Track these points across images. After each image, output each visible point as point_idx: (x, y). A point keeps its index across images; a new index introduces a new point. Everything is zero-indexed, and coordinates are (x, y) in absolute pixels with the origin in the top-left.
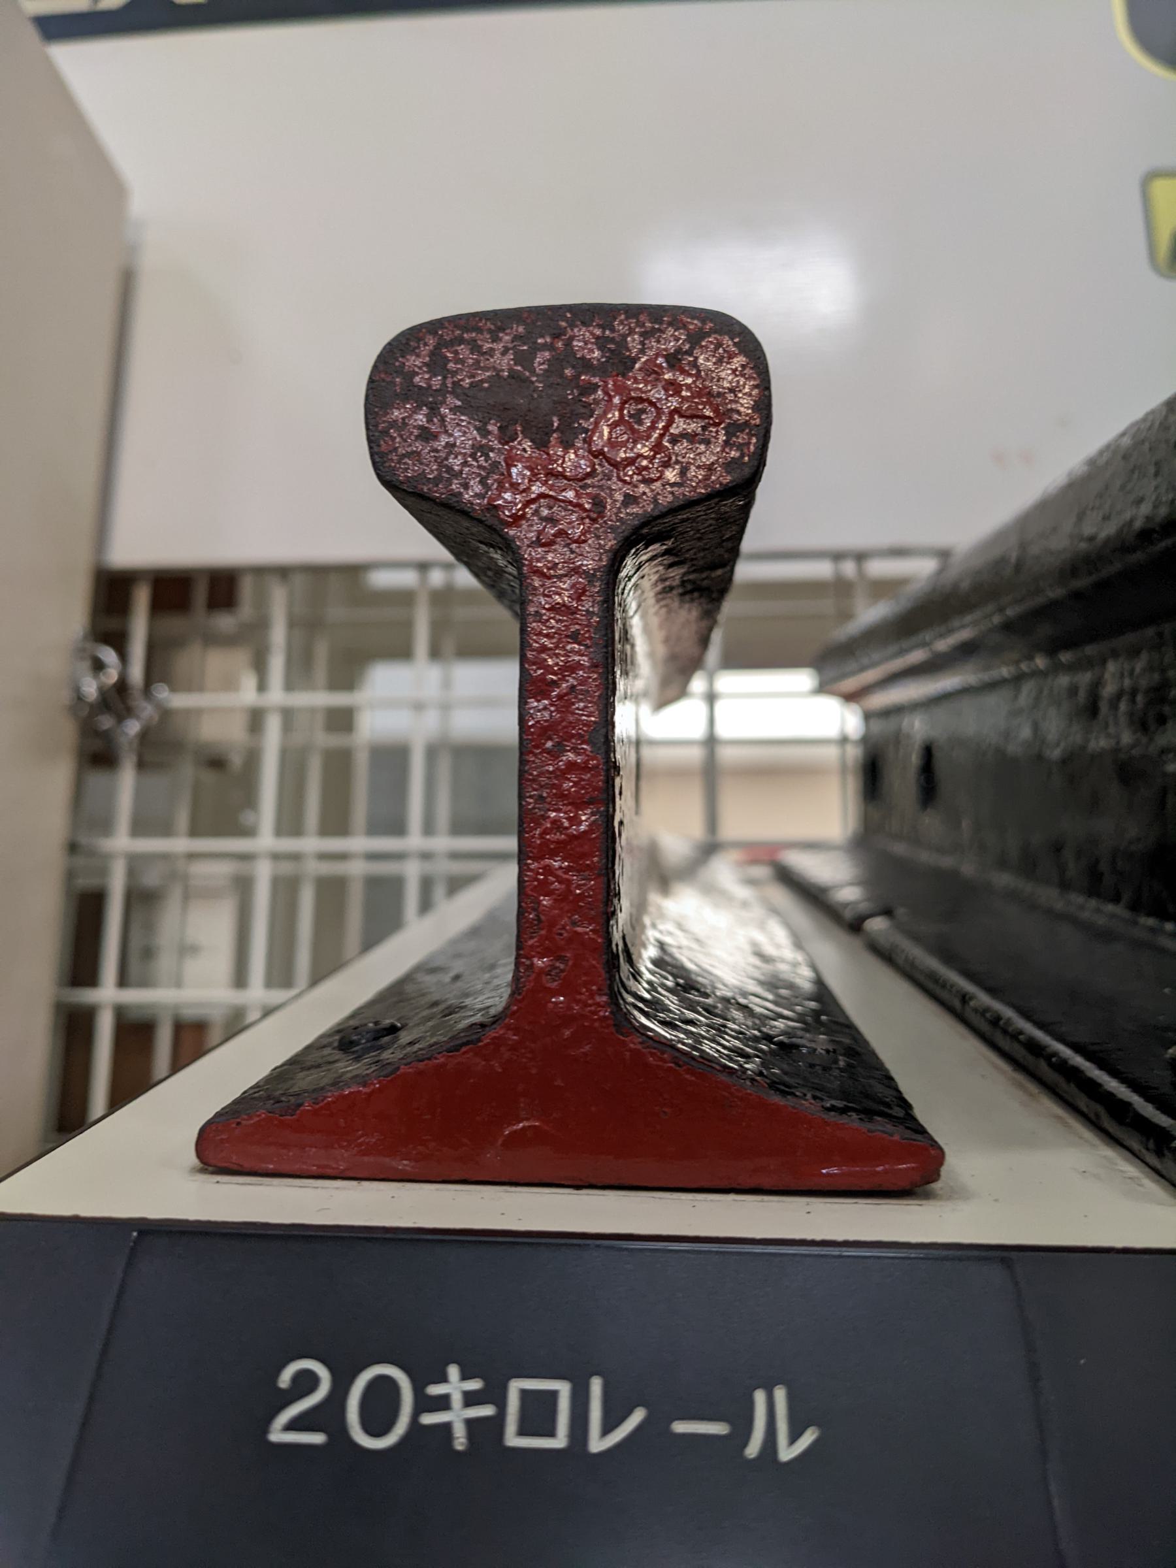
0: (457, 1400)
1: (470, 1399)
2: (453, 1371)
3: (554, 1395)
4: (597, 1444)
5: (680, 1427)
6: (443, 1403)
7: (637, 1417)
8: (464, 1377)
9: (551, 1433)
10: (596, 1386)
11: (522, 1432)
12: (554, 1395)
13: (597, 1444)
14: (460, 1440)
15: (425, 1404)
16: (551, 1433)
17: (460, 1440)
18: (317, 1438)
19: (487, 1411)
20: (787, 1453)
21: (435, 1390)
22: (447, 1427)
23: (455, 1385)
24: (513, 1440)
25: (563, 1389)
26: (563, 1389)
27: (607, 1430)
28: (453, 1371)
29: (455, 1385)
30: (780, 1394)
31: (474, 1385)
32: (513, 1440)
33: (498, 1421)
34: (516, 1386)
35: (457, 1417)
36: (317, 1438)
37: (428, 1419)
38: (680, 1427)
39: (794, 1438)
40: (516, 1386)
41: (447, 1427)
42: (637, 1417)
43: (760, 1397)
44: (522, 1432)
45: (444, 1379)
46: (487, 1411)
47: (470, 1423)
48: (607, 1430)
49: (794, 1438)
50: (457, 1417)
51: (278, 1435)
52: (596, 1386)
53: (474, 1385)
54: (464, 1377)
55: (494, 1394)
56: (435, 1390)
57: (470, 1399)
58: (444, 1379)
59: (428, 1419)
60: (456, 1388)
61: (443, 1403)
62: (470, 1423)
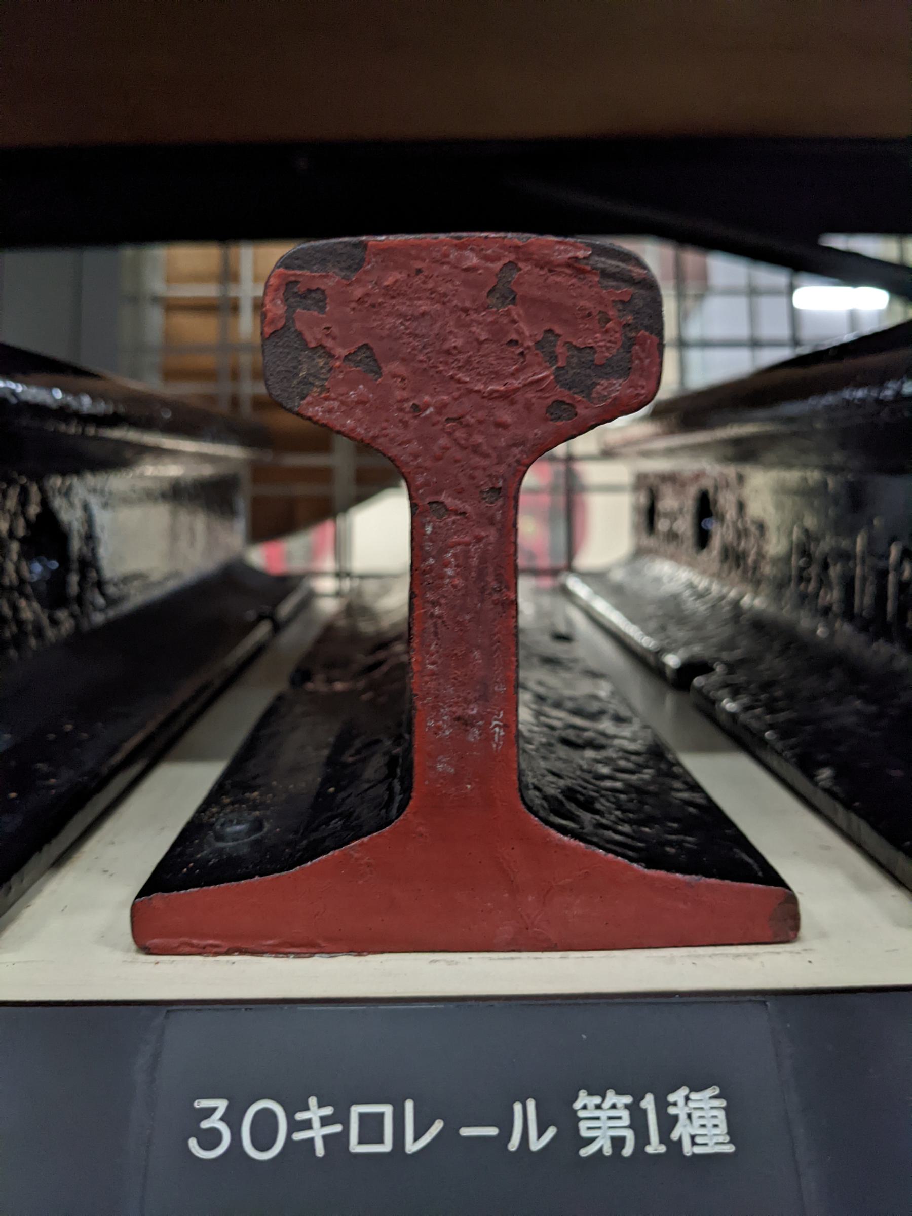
0: (316, 1123)
2: (313, 1101)
6: (307, 1125)
8: (321, 1105)
11: (361, 1141)
12: (381, 1115)
14: (320, 1151)
15: (295, 1126)
17: (320, 1151)
19: (337, 1128)
21: (300, 1116)
22: (311, 1141)
23: (315, 1112)
24: (355, 1147)
25: (387, 1110)
26: (387, 1110)
28: (313, 1101)
29: (315, 1112)
31: (328, 1111)
32: (355, 1147)
34: (356, 1111)
35: (317, 1133)
37: (298, 1136)
40: (356, 1111)
41: (311, 1141)
44: (361, 1141)
45: (306, 1108)
46: (337, 1128)
47: (326, 1138)
50: (317, 1133)
53: (328, 1111)
54: (321, 1105)
55: (341, 1117)
56: (300, 1116)
58: (306, 1108)
59: (298, 1136)
60: (315, 1114)
61: (307, 1125)
62: (326, 1138)
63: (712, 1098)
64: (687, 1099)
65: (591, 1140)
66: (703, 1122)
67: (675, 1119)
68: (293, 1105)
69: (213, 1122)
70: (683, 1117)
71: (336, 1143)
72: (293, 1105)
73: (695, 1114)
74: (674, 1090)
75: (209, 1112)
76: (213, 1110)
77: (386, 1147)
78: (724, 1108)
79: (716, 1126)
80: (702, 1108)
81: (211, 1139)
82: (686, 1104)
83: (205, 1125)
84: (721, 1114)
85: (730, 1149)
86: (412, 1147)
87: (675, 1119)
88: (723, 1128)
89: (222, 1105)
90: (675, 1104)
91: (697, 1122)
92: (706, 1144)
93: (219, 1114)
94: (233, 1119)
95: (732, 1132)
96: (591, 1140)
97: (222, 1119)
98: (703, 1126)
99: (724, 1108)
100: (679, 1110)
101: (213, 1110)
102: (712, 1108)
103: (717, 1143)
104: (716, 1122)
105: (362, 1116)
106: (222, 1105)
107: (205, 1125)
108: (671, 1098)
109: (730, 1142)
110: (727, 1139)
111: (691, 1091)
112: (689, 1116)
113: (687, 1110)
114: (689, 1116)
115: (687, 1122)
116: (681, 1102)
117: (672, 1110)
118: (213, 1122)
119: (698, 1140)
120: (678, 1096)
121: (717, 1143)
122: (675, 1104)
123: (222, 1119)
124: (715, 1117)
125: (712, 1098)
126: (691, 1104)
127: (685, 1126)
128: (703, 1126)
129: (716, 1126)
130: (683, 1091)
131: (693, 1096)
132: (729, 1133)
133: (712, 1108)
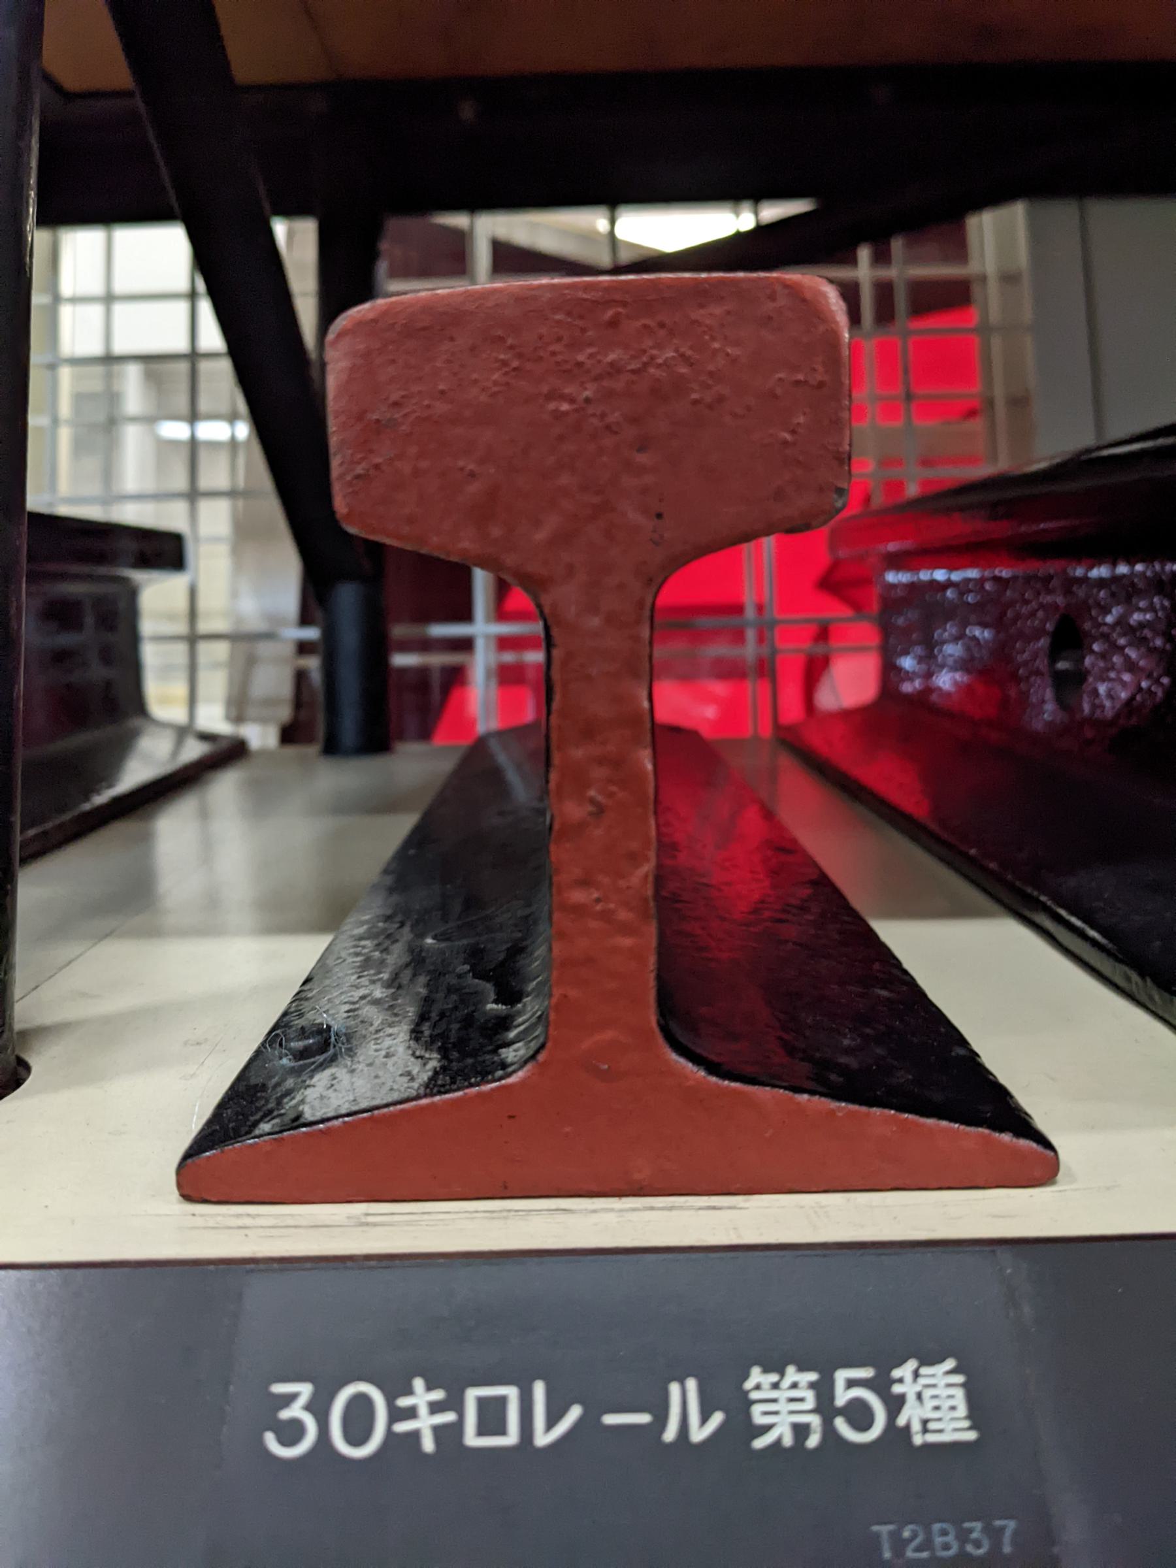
0: (423, 1410)
1: (435, 1408)
2: (418, 1384)
3: (502, 1401)
4: (542, 1439)
5: (610, 1419)
6: (411, 1413)
7: (575, 1412)
8: (429, 1388)
9: (502, 1431)
10: (539, 1390)
13: (542, 1439)
15: (396, 1415)
16: (502, 1431)
19: (449, 1417)
20: (698, 1434)
21: (404, 1402)
23: (421, 1396)
24: (472, 1439)
25: (511, 1393)
26: (511, 1393)
28: (418, 1384)
29: (421, 1396)
30: (692, 1384)
31: (438, 1395)
32: (472, 1439)
33: (459, 1426)
34: (472, 1394)
35: (425, 1424)
37: (402, 1427)
38: (610, 1419)
39: (704, 1419)
40: (472, 1394)
42: (575, 1412)
43: (674, 1389)
44: (481, 1432)
46: (449, 1417)
47: (437, 1430)
49: (704, 1419)
50: (425, 1424)
52: (539, 1390)
53: (438, 1395)
54: (429, 1388)
55: (454, 1403)
56: (404, 1402)
57: (435, 1408)
59: (402, 1427)
61: (411, 1413)
62: (437, 1430)
64: (916, 1374)
66: (935, 1403)
67: (901, 1400)
68: (396, 1387)
69: (295, 1411)
70: (911, 1399)
71: (448, 1435)
72: (396, 1387)
73: (927, 1393)
74: (900, 1363)
75: (291, 1398)
76: (293, 1397)
77: (512, 1438)
78: (964, 1385)
79: (953, 1408)
80: (934, 1386)
81: (291, 1433)
83: (285, 1414)
84: (959, 1394)
85: (971, 1436)
88: (962, 1411)
89: (305, 1390)
90: (900, 1381)
91: (929, 1404)
92: (940, 1431)
93: (302, 1400)
94: (319, 1408)
95: (976, 1416)
97: (308, 1408)
98: (937, 1408)
99: (964, 1385)
100: (907, 1388)
101: (293, 1397)
104: (951, 1402)
106: (305, 1390)
107: (285, 1414)
108: (896, 1373)
109: (970, 1428)
110: (966, 1424)
112: (919, 1396)
113: (918, 1388)
114: (919, 1396)
115: (917, 1403)
116: (908, 1377)
117: (897, 1389)
118: (295, 1411)
119: (932, 1426)
120: (905, 1371)
122: (900, 1381)
123: (308, 1408)
124: (951, 1397)
126: (922, 1381)
128: (937, 1408)
129: (953, 1408)
130: (912, 1365)
131: (924, 1371)
132: (969, 1417)
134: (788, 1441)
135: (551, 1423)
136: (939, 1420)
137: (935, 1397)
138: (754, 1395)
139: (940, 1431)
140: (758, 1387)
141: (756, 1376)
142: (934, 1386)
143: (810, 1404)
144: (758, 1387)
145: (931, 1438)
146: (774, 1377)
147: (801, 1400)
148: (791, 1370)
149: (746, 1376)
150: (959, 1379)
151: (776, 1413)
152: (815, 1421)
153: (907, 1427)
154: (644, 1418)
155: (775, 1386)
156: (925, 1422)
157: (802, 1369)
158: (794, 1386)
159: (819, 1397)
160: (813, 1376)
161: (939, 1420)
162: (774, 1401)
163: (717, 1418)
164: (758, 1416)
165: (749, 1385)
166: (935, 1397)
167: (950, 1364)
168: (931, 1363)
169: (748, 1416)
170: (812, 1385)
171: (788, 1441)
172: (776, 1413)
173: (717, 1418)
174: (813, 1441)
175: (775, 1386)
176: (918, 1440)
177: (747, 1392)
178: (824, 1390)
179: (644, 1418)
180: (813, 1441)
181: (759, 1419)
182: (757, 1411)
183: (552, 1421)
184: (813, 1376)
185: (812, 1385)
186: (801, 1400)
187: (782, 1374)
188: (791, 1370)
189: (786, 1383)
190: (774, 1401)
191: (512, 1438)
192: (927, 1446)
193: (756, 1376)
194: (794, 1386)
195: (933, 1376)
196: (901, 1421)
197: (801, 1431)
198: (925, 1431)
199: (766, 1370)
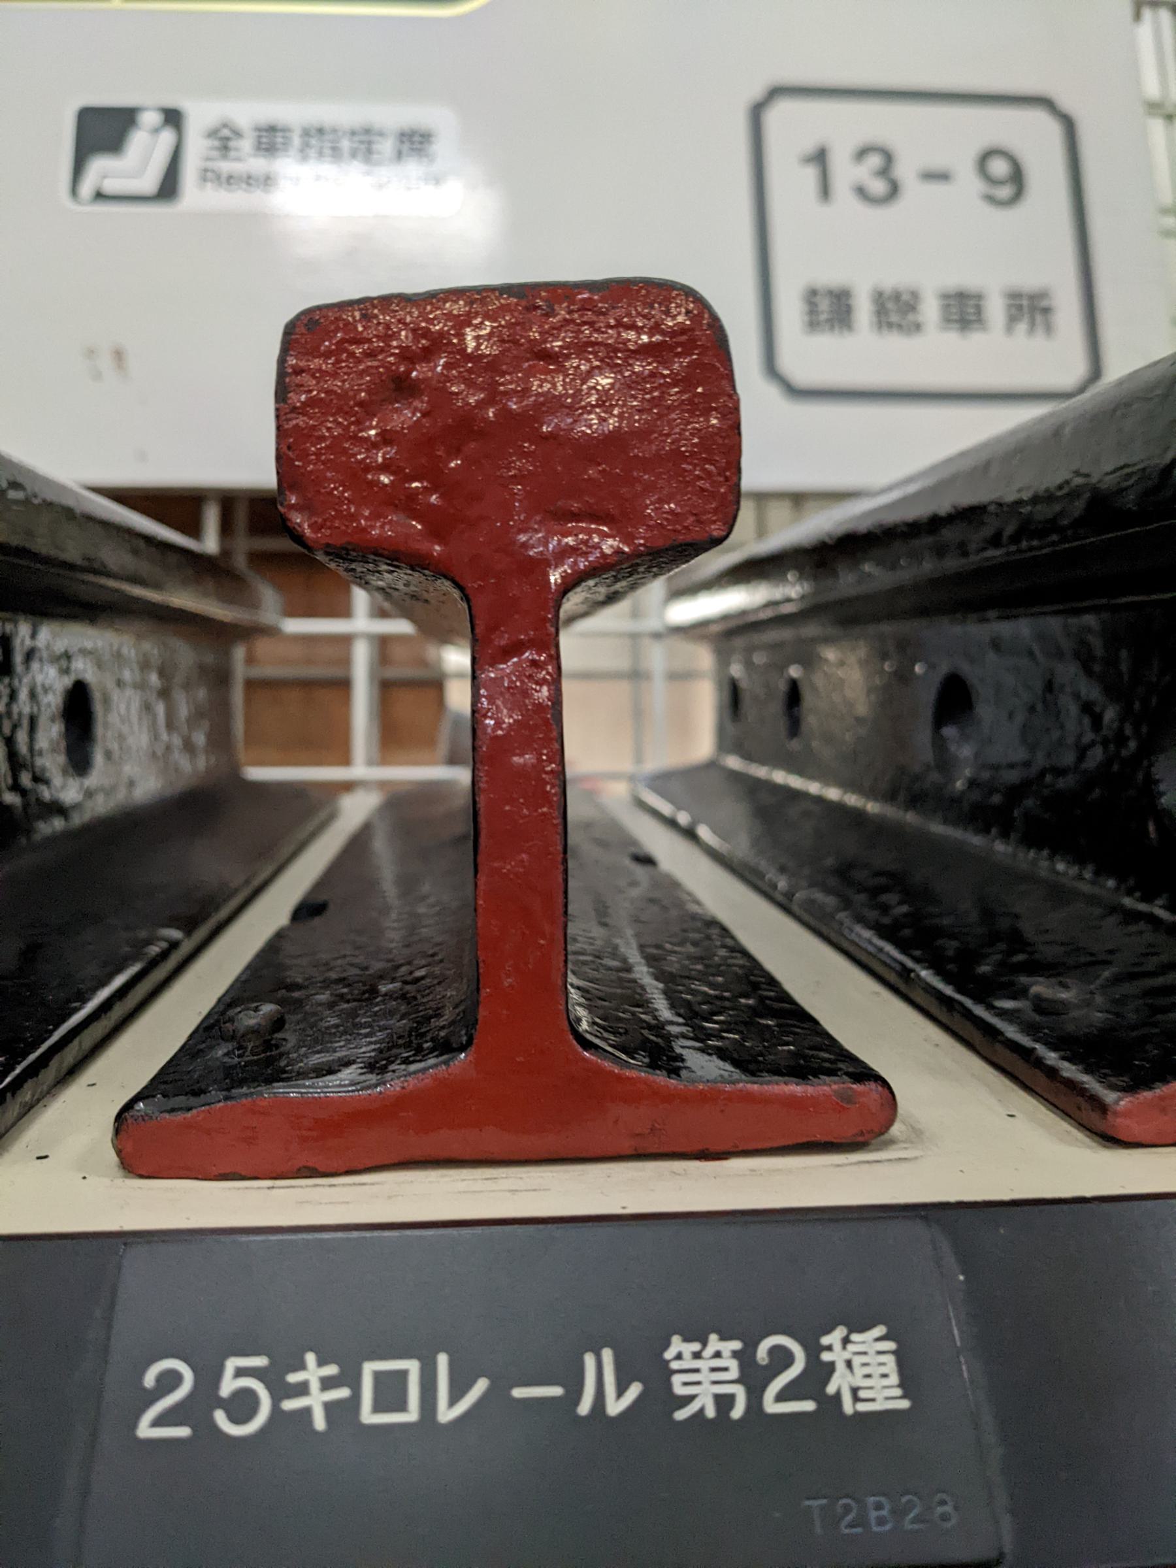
0: (315, 1386)
1: (327, 1384)
2: (311, 1358)
3: (404, 1374)
5: (518, 1393)
6: (302, 1389)
7: (481, 1386)
8: (321, 1363)
9: (402, 1407)
10: (443, 1360)
11: (378, 1408)
12: (404, 1374)
14: (319, 1422)
16: (402, 1407)
17: (319, 1422)
18: (183, 1432)
19: (343, 1393)
21: (293, 1378)
22: (307, 1412)
23: (312, 1371)
24: (368, 1416)
25: (412, 1367)
26: (412, 1367)
27: (453, 1401)
28: (311, 1358)
29: (312, 1371)
30: (607, 1355)
31: (331, 1370)
32: (368, 1416)
34: (369, 1368)
35: (316, 1401)
36: (183, 1432)
37: (289, 1405)
38: (518, 1393)
39: (620, 1392)
40: (369, 1368)
41: (307, 1412)
42: (481, 1386)
43: (589, 1360)
44: (378, 1408)
45: (302, 1366)
46: (343, 1393)
47: (329, 1407)
48: (453, 1401)
49: (620, 1392)
50: (316, 1401)
51: (145, 1430)
52: (443, 1360)
53: (331, 1370)
54: (321, 1363)
55: (350, 1378)
56: (293, 1378)
57: (327, 1384)
58: (302, 1366)
59: (289, 1405)
61: (302, 1389)
62: (329, 1407)
63: (878, 1339)
64: (846, 1341)
65: (691, 1398)
66: (866, 1370)
67: (831, 1367)
70: (840, 1367)
73: (857, 1361)
74: (828, 1331)
77: (411, 1415)
79: (885, 1376)
80: (865, 1353)
82: (844, 1348)
84: (890, 1360)
85: (905, 1404)
86: (446, 1414)
87: (831, 1367)
88: (894, 1379)
90: (829, 1348)
91: (859, 1371)
92: (873, 1400)
95: (907, 1384)
96: (691, 1398)
98: (868, 1376)
102: (880, 1353)
103: (887, 1398)
104: (884, 1370)
105: (378, 1376)
108: (825, 1340)
110: (898, 1392)
111: (851, 1331)
112: (849, 1364)
113: (847, 1355)
114: (849, 1364)
115: (847, 1372)
116: (837, 1346)
117: (826, 1357)
119: (862, 1394)
120: (834, 1338)
121: (887, 1398)
122: (829, 1348)
125: (878, 1339)
126: (851, 1348)
127: (843, 1376)
128: (868, 1376)
129: (885, 1376)
130: (839, 1332)
131: (855, 1337)
133: (880, 1353)
134: (710, 1413)
135: (455, 1397)
136: (871, 1388)
137: (865, 1365)
138: (675, 1365)
139: (873, 1400)
140: (679, 1357)
141: (677, 1345)
142: (865, 1353)
143: (734, 1373)
144: (679, 1357)
145: (862, 1407)
146: (696, 1347)
147: (726, 1369)
148: (713, 1340)
149: (667, 1345)
150: (890, 1345)
151: (698, 1383)
152: (740, 1392)
153: (838, 1396)
154: (556, 1391)
155: (697, 1355)
156: (855, 1391)
157: (723, 1338)
158: (718, 1355)
159: (742, 1368)
160: (736, 1345)
161: (871, 1388)
162: (697, 1371)
163: (634, 1390)
164: (678, 1386)
165: (669, 1354)
166: (865, 1365)
167: (879, 1331)
168: (862, 1329)
169: (669, 1386)
170: (735, 1354)
171: (710, 1413)
172: (698, 1383)
173: (634, 1390)
174: (737, 1412)
175: (697, 1355)
176: (848, 1407)
177: (668, 1362)
178: (745, 1357)
179: (556, 1391)
180: (737, 1412)
181: (679, 1390)
182: (677, 1380)
183: (455, 1397)
184: (736, 1345)
185: (735, 1354)
186: (726, 1369)
187: (705, 1344)
188: (713, 1337)
189: (709, 1351)
190: (697, 1371)
191: (411, 1415)
192: (857, 1414)
193: (677, 1345)
194: (718, 1355)
195: (863, 1342)
196: (831, 1389)
197: (724, 1402)
198: (856, 1399)
199: (687, 1339)
